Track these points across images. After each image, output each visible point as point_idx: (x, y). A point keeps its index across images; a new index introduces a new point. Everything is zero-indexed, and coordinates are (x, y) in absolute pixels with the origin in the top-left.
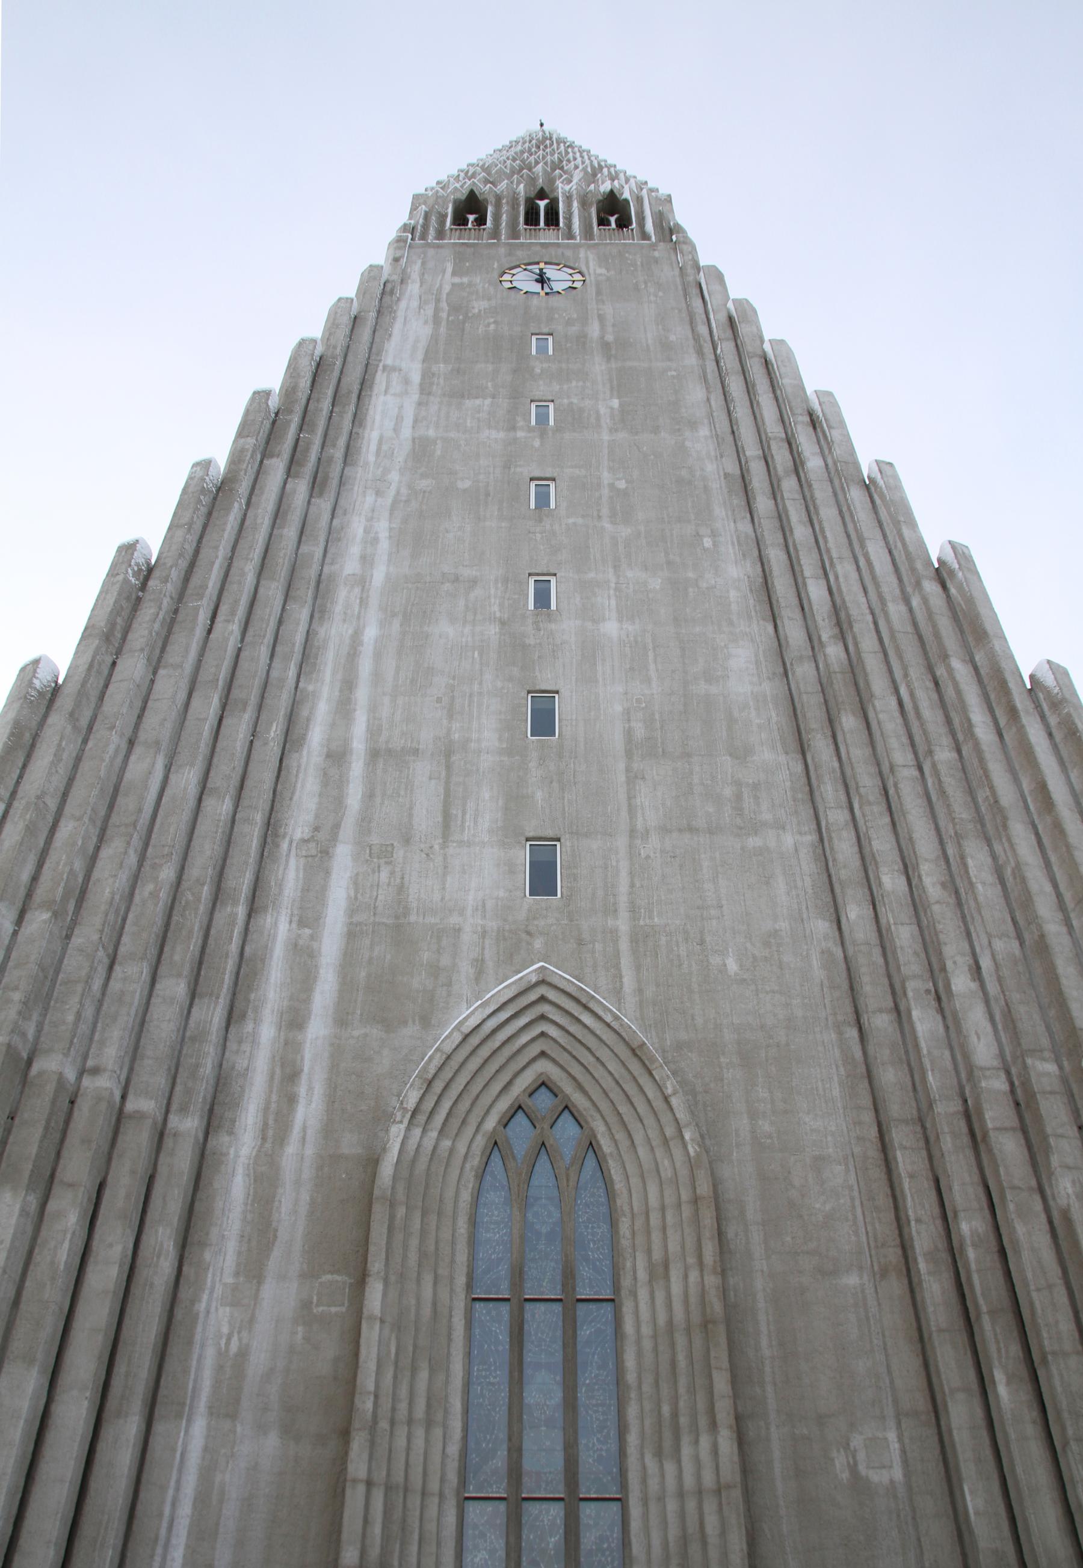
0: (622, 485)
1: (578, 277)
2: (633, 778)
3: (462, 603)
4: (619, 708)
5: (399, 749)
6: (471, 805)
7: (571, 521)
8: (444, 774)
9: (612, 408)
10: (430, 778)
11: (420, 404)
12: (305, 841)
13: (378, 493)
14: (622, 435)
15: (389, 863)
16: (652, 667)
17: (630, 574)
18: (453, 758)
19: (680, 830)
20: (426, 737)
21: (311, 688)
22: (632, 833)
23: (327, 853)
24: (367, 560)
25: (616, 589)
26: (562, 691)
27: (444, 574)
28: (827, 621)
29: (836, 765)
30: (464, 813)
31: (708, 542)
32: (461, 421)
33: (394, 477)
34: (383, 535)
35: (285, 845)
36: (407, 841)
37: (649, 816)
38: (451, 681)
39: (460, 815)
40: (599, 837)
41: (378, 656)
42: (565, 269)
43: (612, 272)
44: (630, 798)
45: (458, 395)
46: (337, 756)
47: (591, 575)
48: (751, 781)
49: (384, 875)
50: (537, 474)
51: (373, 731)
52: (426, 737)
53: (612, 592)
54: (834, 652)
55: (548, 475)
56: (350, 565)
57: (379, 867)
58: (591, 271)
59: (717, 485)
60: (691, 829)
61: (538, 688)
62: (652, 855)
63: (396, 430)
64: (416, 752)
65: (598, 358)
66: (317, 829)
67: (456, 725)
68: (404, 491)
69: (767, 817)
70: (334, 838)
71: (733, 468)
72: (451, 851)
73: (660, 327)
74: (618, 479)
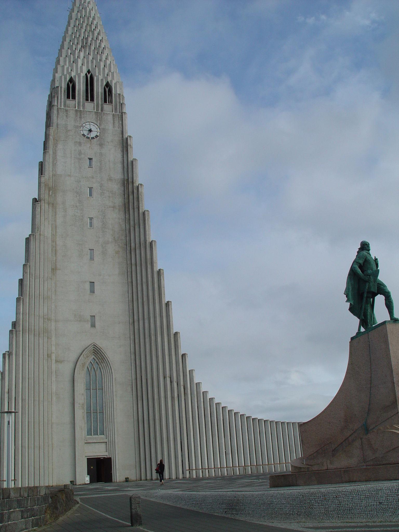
1: (98, 129)
42: (96, 125)
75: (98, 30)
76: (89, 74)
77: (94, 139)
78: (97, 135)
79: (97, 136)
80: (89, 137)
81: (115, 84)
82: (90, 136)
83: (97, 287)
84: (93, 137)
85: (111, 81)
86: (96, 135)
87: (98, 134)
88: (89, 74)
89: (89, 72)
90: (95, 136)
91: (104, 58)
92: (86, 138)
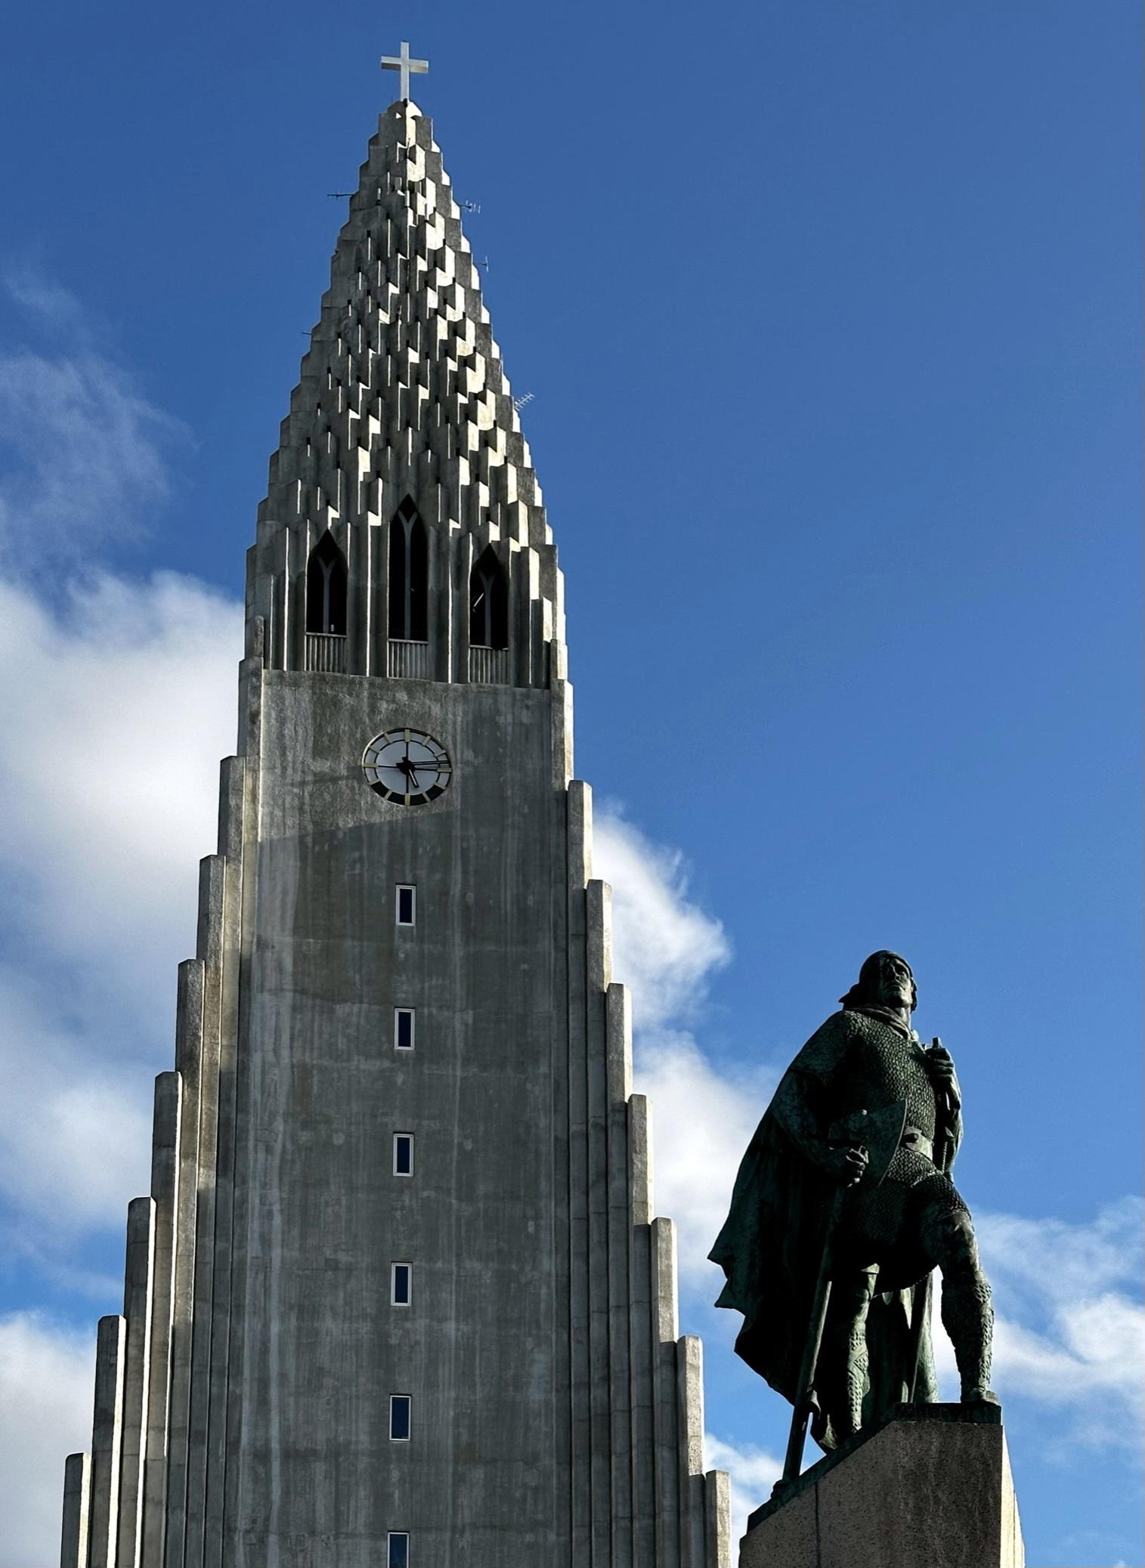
0: (469, 1146)
2: (459, 1479)
3: (341, 1295)
4: (452, 1413)
5: (303, 1449)
6: (352, 1502)
7: (425, 1194)
8: (334, 1473)
9: (467, 1025)
10: (326, 1478)
11: (295, 1009)
12: (247, 1532)
13: (269, 1150)
14: (474, 1070)
15: (302, 1551)
16: (477, 1372)
17: (468, 1264)
18: (341, 1460)
19: (485, 1527)
20: (321, 1446)
21: (238, 1391)
22: (454, 1528)
23: (263, 1542)
24: (265, 1242)
25: (458, 1283)
26: (414, 1395)
27: (327, 1260)
28: (600, 1361)
29: (587, 1489)
30: (349, 1509)
31: (531, 1229)
32: (333, 1040)
33: (279, 1125)
34: (276, 1208)
35: (236, 1538)
36: (313, 1533)
37: (466, 1516)
38: (336, 1383)
39: (346, 1511)
40: (434, 1531)
41: (281, 1353)
43: (480, 760)
44: (455, 1498)
45: (330, 997)
46: (262, 1456)
47: (439, 1265)
48: (533, 1485)
49: (300, 1560)
50: (399, 1128)
51: (285, 1431)
52: (321, 1446)
53: (454, 1287)
54: (598, 1393)
55: (408, 1130)
56: (253, 1248)
57: (297, 1554)
58: (459, 757)
59: (547, 1149)
60: (493, 1527)
61: (397, 1392)
62: (466, 1547)
63: (276, 1052)
64: (314, 1452)
65: (458, 938)
66: (254, 1522)
67: (341, 1428)
68: (289, 1145)
69: (540, 1517)
70: (266, 1530)
71: (563, 1136)
72: (342, 1541)
73: (521, 879)
74: (466, 1137)
75: (454, 315)
76: (408, 521)
77: (426, 802)
78: (437, 785)
79: (435, 792)
80: (404, 796)
81: (522, 557)
82: (407, 792)
83: (415, 1414)
84: (421, 795)
85: (503, 545)
86: (435, 787)
87: (442, 783)
88: (408, 521)
89: (406, 509)
90: (427, 792)
91: (473, 444)
92: (390, 799)
